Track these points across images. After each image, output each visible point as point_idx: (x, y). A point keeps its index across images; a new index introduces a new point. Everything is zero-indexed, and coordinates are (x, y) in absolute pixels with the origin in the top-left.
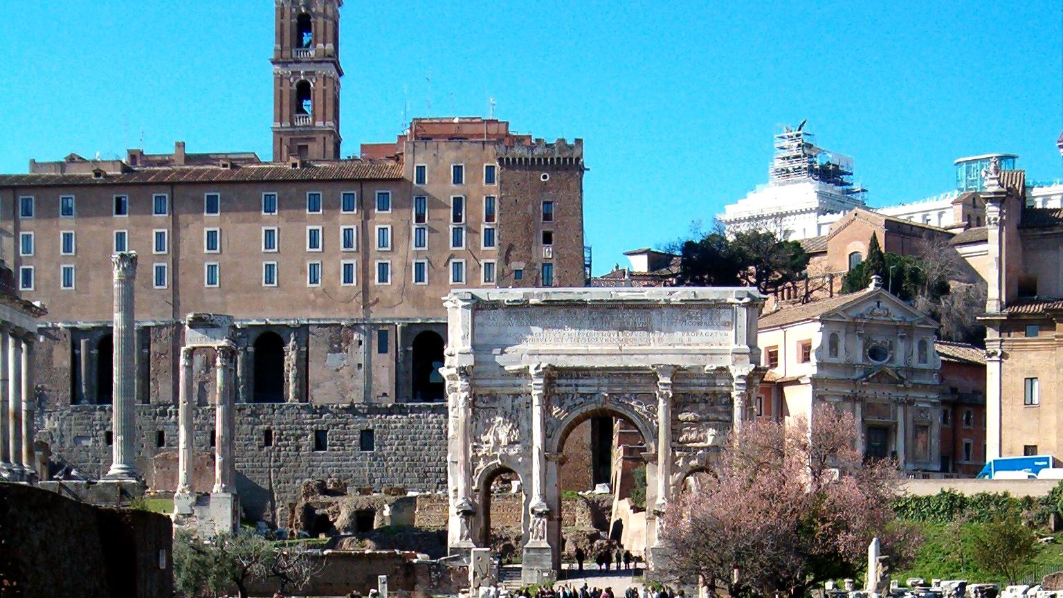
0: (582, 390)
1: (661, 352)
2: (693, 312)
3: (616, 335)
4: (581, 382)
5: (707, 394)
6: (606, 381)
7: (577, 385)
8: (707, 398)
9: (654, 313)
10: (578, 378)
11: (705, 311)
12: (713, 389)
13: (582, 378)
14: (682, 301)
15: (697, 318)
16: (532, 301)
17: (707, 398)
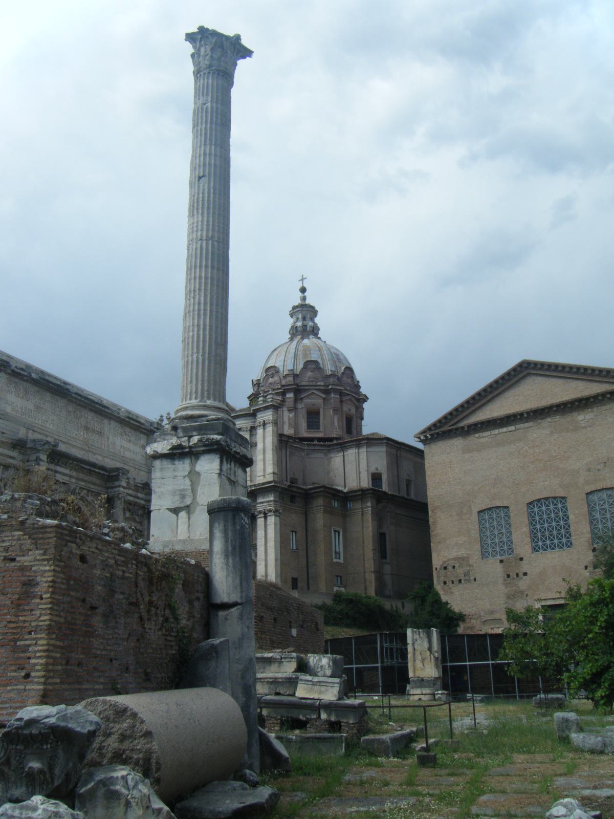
0: (59, 477)
1: (112, 457)
2: (128, 430)
3: (82, 434)
4: (59, 469)
5: (130, 504)
6: (74, 474)
7: (56, 472)
8: (131, 507)
9: (106, 421)
10: (57, 464)
11: (133, 432)
12: (136, 500)
13: (60, 466)
14: (128, 417)
15: (129, 436)
16: (34, 375)
17: (131, 507)
